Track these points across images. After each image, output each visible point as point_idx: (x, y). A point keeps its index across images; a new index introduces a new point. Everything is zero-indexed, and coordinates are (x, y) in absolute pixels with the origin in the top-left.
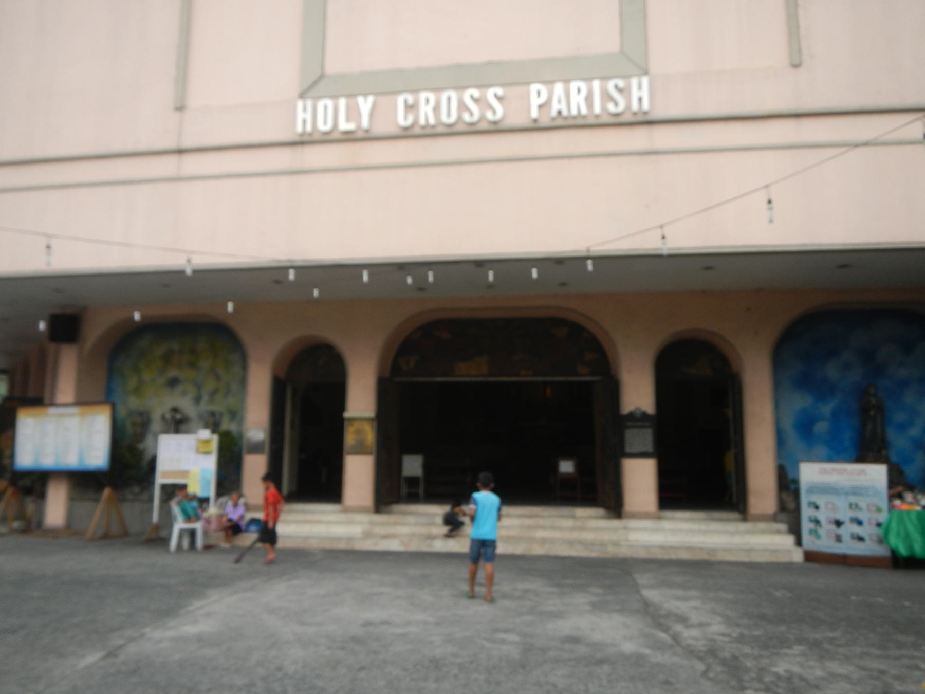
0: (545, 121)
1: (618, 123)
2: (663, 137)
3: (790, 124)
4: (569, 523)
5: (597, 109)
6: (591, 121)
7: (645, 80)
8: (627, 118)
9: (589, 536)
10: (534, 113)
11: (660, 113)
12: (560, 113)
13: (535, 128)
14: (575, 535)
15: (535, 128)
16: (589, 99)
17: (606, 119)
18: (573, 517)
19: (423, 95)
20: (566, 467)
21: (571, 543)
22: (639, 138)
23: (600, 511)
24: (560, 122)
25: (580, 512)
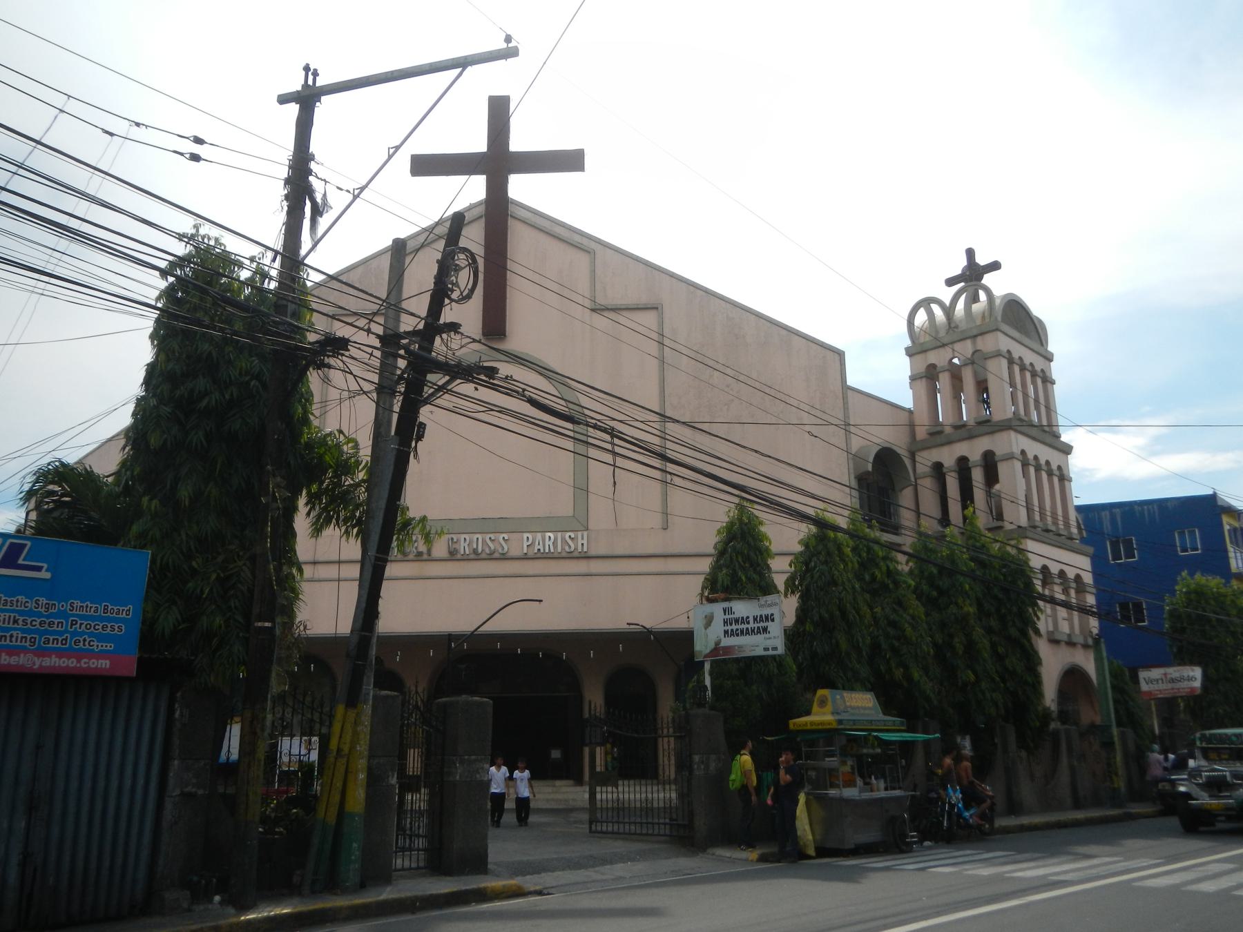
0: (531, 554)
1: (571, 556)
2: (596, 566)
3: (662, 560)
4: (550, 789)
5: (559, 550)
6: (556, 555)
7: (585, 533)
8: (576, 554)
9: (560, 796)
10: (525, 551)
11: (593, 552)
12: (539, 550)
13: (525, 558)
14: (552, 796)
15: (525, 558)
16: (555, 543)
17: (564, 554)
18: (554, 786)
19: (463, 536)
20: (556, 754)
21: (548, 800)
22: (581, 566)
23: (571, 782)
24: (539, 555)
25: (558, 783)
